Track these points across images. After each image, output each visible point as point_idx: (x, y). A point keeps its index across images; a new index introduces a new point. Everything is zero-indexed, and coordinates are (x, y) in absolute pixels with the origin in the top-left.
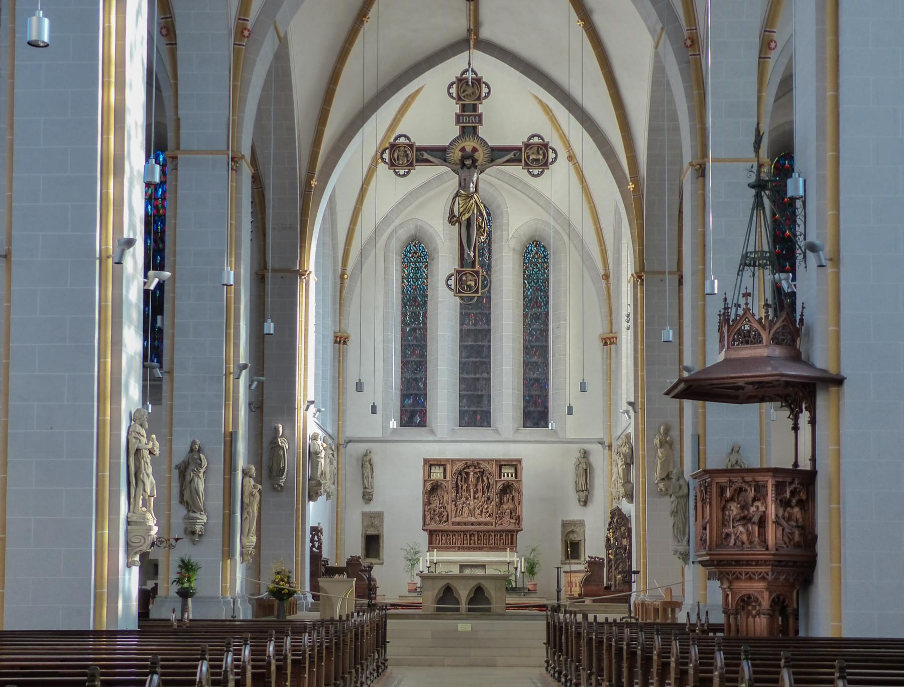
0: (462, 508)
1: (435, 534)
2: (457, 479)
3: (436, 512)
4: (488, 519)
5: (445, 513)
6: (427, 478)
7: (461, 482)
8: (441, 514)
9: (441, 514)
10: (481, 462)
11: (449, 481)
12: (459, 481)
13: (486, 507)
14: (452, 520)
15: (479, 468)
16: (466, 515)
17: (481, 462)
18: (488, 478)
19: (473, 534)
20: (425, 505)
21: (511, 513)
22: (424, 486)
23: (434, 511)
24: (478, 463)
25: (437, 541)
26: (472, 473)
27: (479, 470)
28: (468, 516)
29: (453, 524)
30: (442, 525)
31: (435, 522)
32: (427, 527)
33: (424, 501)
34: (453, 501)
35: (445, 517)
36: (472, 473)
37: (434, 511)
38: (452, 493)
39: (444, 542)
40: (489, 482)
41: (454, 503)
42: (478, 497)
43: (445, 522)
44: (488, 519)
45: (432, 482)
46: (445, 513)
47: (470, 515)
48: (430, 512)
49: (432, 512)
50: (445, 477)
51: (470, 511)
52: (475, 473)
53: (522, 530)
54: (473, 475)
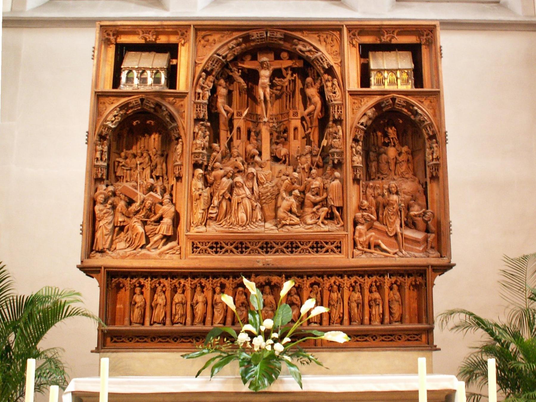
0: (231, 189)
1: (128, 282)
2: (214, 91)
3: (134, 207)
4: (326, 228)
5: (167, 210)
6: (107, 86)
7: (230, 104)
8: (151, 210)
9: (151, 210)
10: (298, 34)
11: (183, 95)
12: (221, 102)
13: (317, 183)
14: (194, 231)
15: (293, 56)
16: (242, 215)
17: (298, 34)
18: (321, 92)
19: (268, 283)
20: (98, 180)
21: (408, 208)
22: (97, 112)
23: (130, 202)
24: (287, 38)
25: (137, 312)
26: (265, 75)
27: (289, 63)
28: (251, 219)
29: (194, 247)
30: (154, 253)
31: (131, 243)
32: (98, 261)
33: (92, 167)
34: (196, 166)
35: (167, 221)
36: (265, 75)
37: (130, 202)
38: (195, 136)
39: (159, 313)
40: (326, 106)
41: (200, 171)
43: (168, 239)
44: (326, 228)
45: (123, 100)
46: (167, 210)
47: (259, 215)
48: (114, 207)
49: (121, 204)
50: (172, 81)
51: (259, 199)
52: (277, 73)
53: (449, 267)
54: (272, 78)
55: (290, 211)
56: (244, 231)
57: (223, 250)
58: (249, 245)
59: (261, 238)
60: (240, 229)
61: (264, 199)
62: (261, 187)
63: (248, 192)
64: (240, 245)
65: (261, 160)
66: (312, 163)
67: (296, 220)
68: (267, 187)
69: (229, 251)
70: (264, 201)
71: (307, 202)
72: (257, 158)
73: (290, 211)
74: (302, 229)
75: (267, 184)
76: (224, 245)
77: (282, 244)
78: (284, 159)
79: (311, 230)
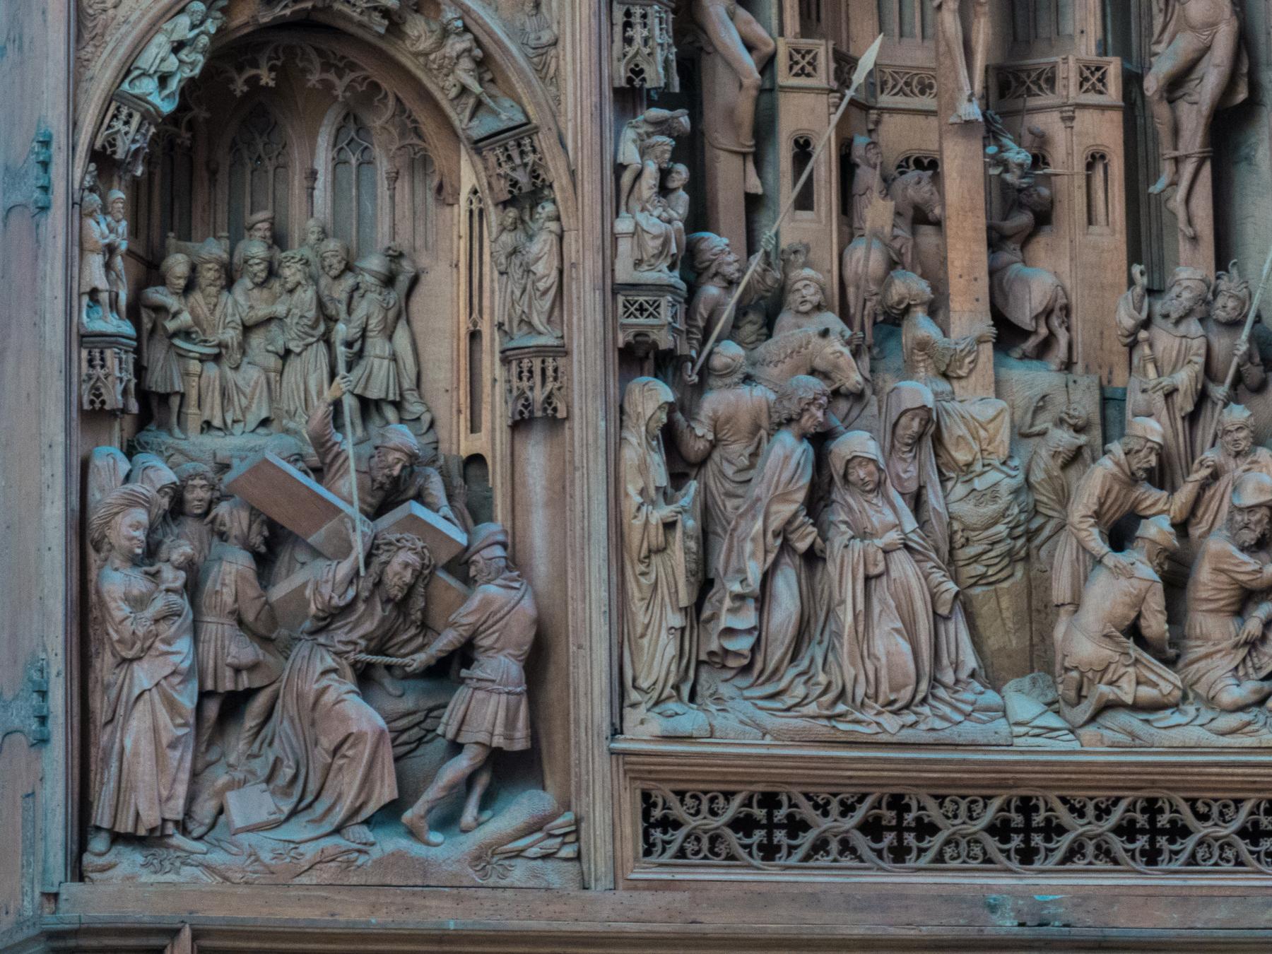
42: (1056, 310)
55: (1134, 631)
56: (908, 735)
57: (806, 840)
58: (934, 813)
59: (1000, 778)
60: (891, 723)
61: (976, 558)
62: (960, 490)
63: (910, 523)
64: (889, 816)
65: (946, 333)
66: (1209, 372)
67: (1167, 682)
68: (992, 493)
69: (834, 846)
70: (978, 569)
71: (1205, 578)
72: (921, 326)
73: (1134, 631)
74: (1194, 734)
75: (993, 476)
76: (807, 811)
77: (1102, 812)
78: (1043, 331)
79: (1248, 741)
